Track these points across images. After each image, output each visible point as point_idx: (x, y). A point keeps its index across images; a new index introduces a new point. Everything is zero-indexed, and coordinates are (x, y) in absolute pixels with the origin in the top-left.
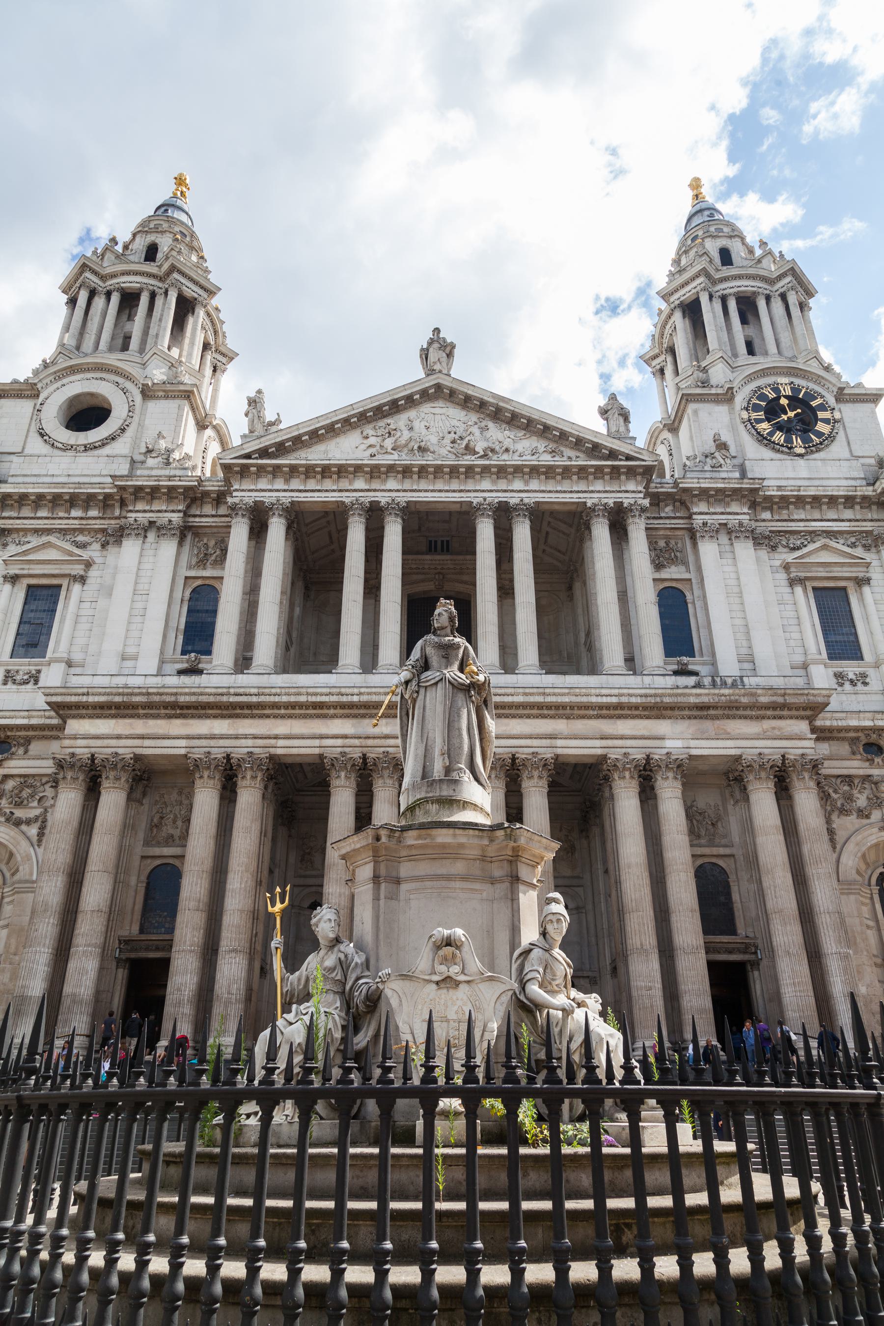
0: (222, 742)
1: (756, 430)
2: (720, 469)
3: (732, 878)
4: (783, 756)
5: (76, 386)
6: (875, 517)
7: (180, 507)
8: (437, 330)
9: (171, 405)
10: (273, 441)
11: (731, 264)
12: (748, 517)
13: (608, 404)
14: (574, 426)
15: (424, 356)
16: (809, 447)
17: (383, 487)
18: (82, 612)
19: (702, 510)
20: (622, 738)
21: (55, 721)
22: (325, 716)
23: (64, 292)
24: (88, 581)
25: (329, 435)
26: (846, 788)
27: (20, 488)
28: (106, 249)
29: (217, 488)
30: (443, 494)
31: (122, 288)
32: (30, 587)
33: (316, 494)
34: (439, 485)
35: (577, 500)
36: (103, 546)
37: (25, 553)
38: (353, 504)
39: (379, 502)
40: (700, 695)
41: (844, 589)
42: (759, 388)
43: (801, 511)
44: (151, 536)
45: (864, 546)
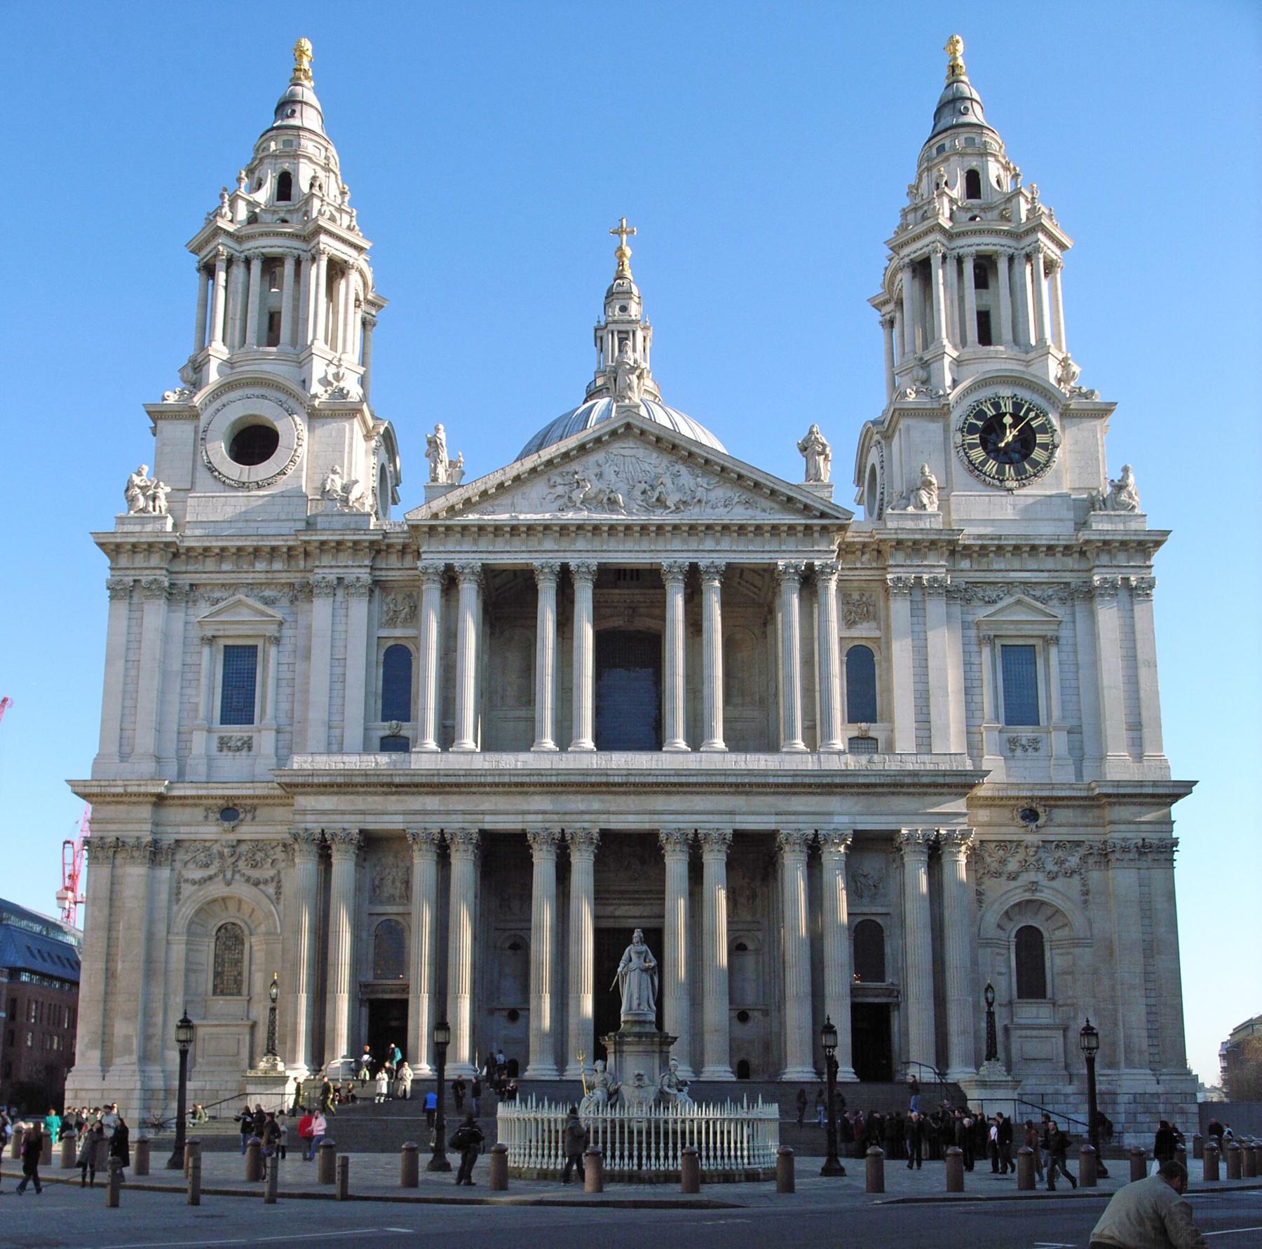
0: (435, 818)
1: (968, 457)
3: (886, 933)
6: (1076, 567)
7: (367, 562)
12: (944, 570)
16: (1022, 479)
17: (573, 548)
18: (282, 676)
20: (795, 813)
21: (279, 792)
22: (526, 793)
23: (195, 251)
26: (1001, 852)
27: (204, 541)
29: (402, 540)
30: (632, 555)
31: (262, 254)
32: (226, 647)
33: (506, 556)
34: (629, 545)
35: (768, 561)
37: (218, 613)
42: (979, 403)
43: (1002, 559)
44: (340, 592)
45: (1061, 599)
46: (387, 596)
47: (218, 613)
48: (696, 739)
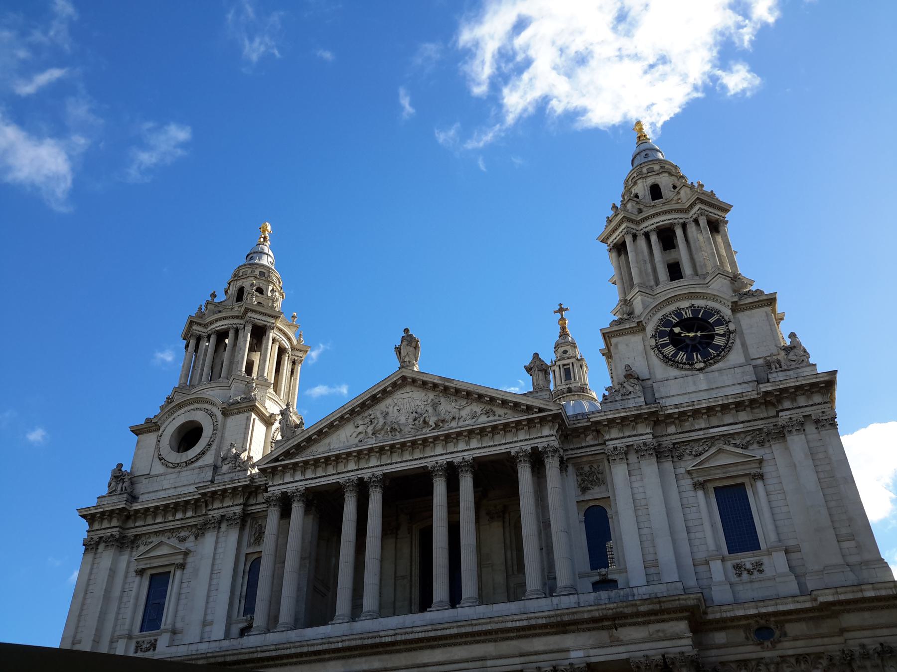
1: (662, 354)
2: (630, 396)
4: (663, 656)
5: (181, 418)
7: (241, 501)
8: (406, 330)
9: (241, 417)
10: (292, 445)
11: (662, 198)
13: (531, 363)
14: (498, 392)
15: (398, 353)
16: (708, 360)
19: (613, 436)
20: (536, 653)
23: (184, 339)
24: (187, 567)
25: (332, 430)
27: (144, 505)
28: (208, 303)
30: (408, 464)
32: (152, 576)
33: (323, 479)
35: (505, 451)
36: (196, 538)
37: (148, 552)
38: (347, 483)
39: (362, 478)
40: (592, 611)
41: (743, 484)
44: (224, 526)
45: (758, 443)
46: (255, 524)
47: (148, 552)
48: (455, 598)
